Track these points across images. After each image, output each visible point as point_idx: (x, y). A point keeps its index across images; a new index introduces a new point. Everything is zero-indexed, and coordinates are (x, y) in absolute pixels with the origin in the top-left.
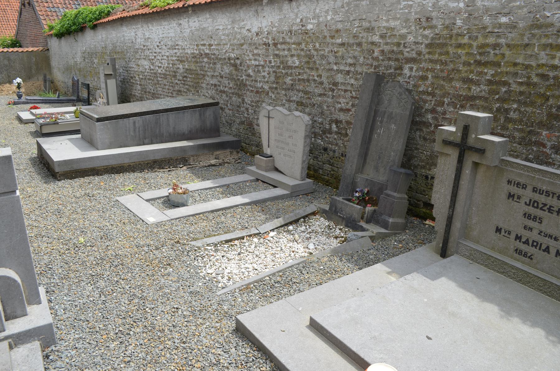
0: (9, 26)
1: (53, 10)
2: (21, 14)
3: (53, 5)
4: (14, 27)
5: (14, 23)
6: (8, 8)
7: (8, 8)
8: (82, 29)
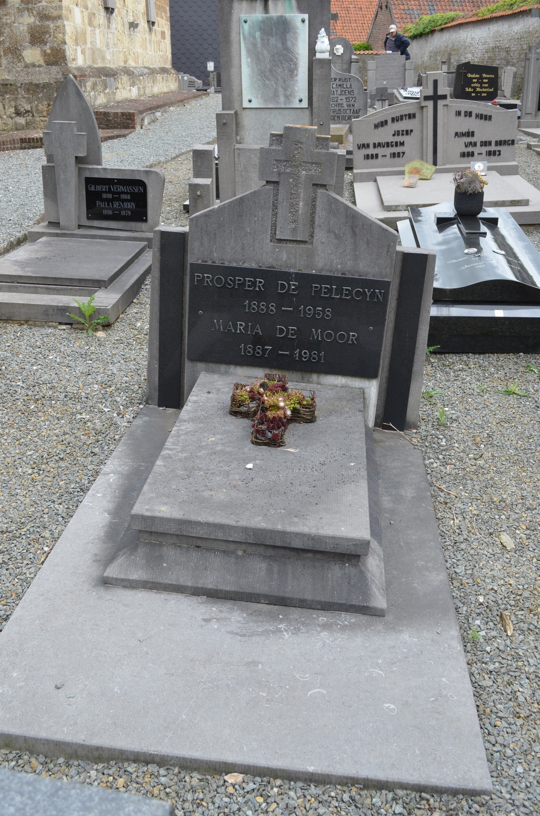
0: (350, 28)
1: (408, 12)
2: (376, 16)
4: (355, 30)
5: (355, 25)
6: (351, 6)
7: (351, 6)
8: (432, 32)
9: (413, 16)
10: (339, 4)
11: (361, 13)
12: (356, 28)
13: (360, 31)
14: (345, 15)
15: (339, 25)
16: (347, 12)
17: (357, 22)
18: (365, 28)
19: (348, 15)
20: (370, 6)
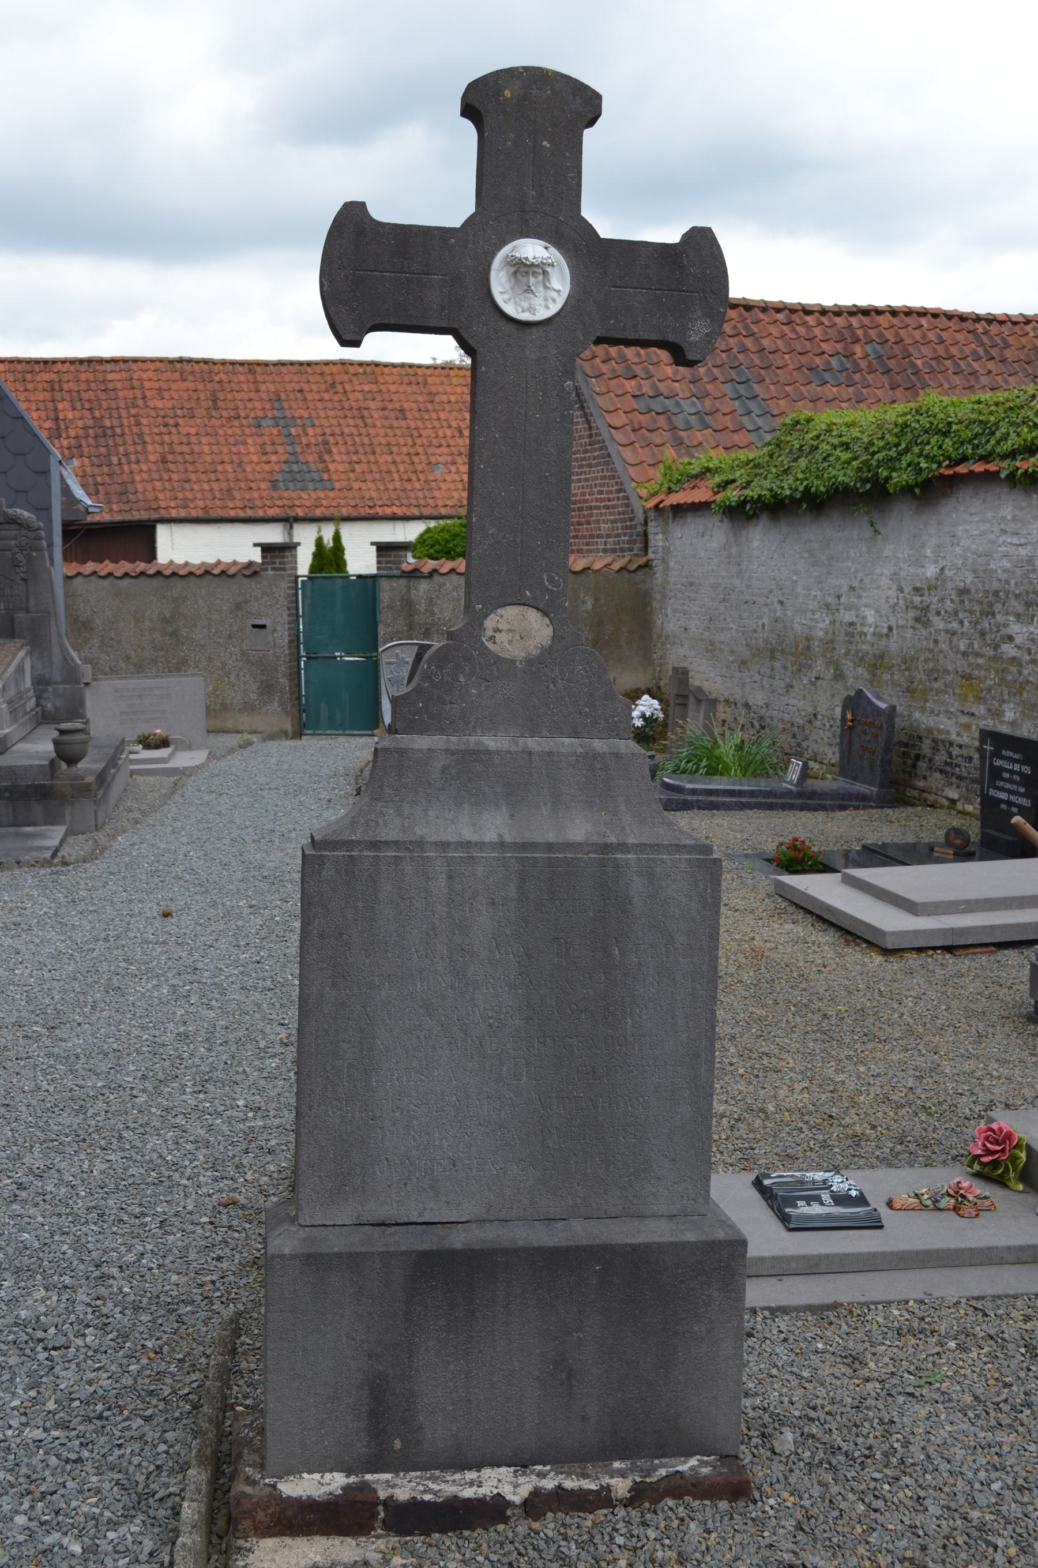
0: (374, 468)
3: (654, 386)
4: (389, 472)
5: (389, 459)
6: (372, 405)
7: (372, 405)
9: (679, 421)
10: (336, 398)
11: (403, 424)
12: (393, 468)
13: (405, 477)
14: (354, 431)
15: (337, 458)
16: (359, 422)
17: (395, 449)
18: (419, 468)
19: (363, 431)
20: (430, 406)
